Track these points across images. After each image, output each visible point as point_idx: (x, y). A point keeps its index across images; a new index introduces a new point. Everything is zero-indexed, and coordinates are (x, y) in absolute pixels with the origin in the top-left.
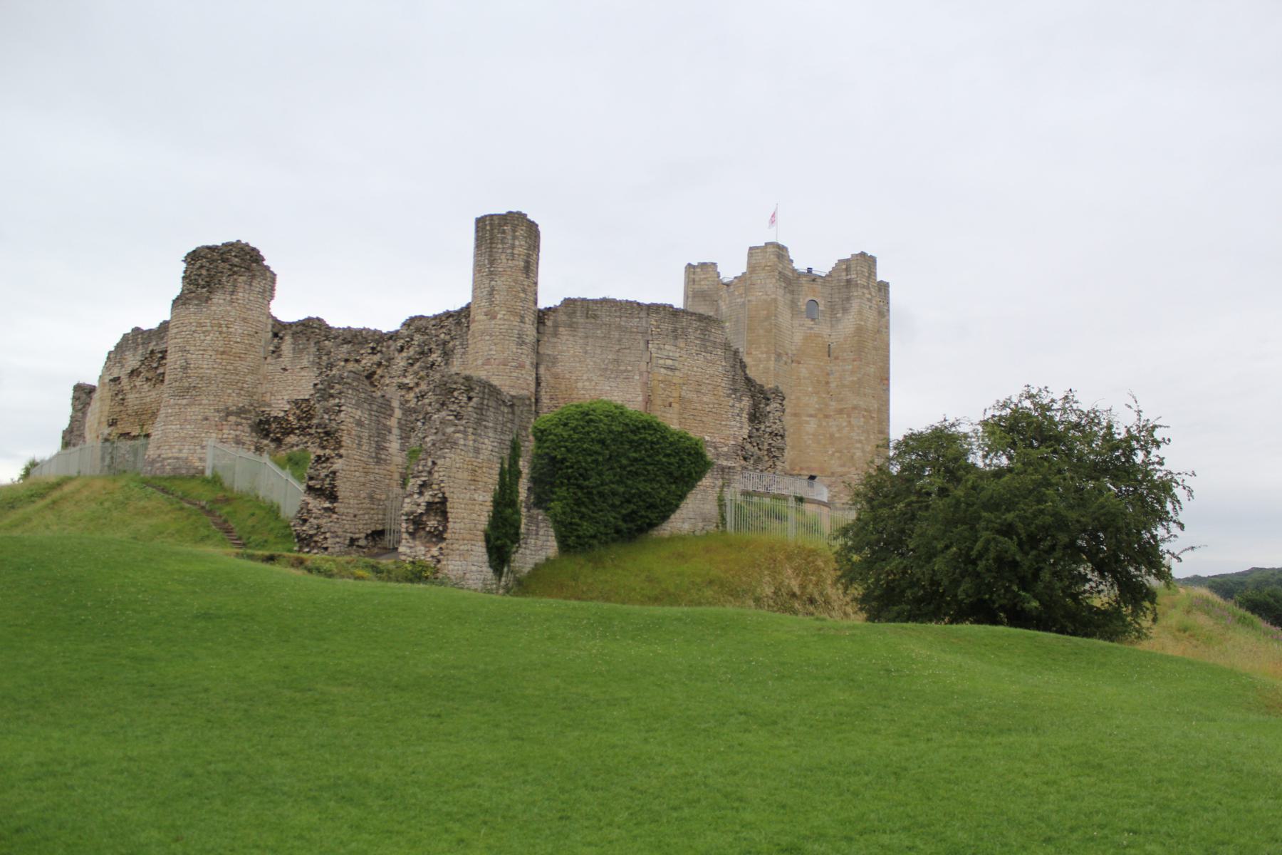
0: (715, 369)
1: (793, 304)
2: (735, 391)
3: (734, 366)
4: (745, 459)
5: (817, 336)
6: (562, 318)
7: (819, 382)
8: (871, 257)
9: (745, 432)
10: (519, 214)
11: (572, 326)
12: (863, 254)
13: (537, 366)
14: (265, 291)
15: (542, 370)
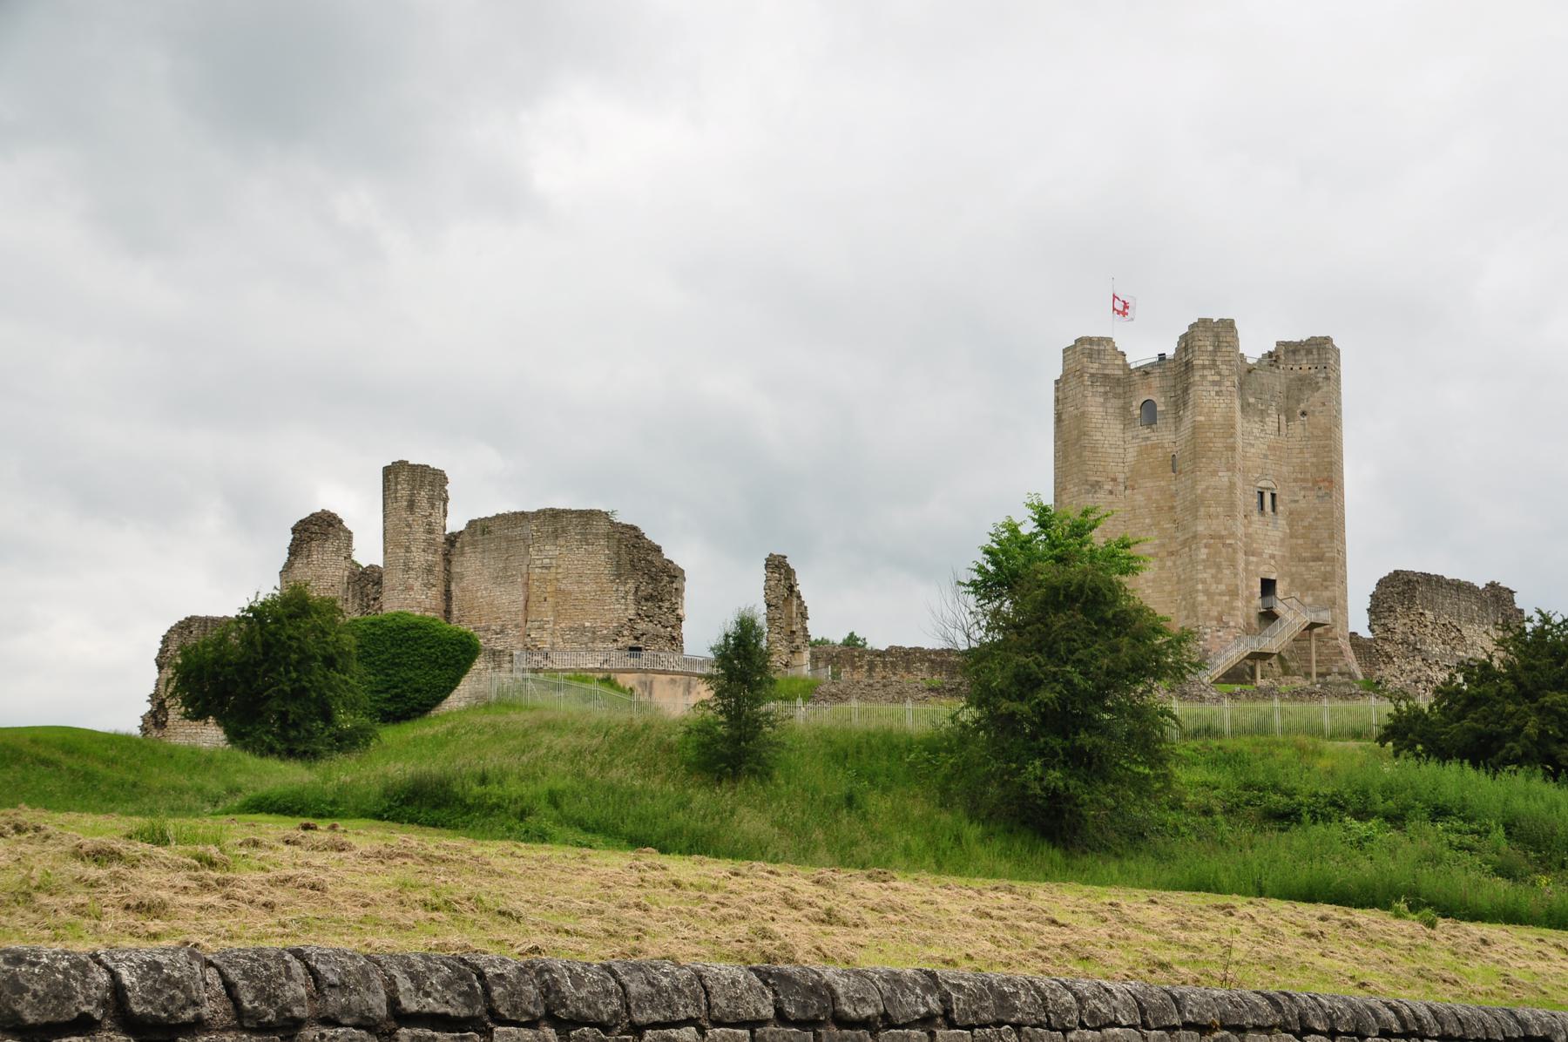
0: (598, 559)
1: (1125, 409)
2: (619, 576)
3: (618, 554)
4: (637, 638)
5: (1154, 447)
6: (467, 538)
7: (1159, 509)
8: (1221, 320)
9: (631, 613)
10: (401, 462)
11: (474, 544)
12: (1204, 323)
13: (448, 583)
14: (339, 549)
15: (453, 586)
